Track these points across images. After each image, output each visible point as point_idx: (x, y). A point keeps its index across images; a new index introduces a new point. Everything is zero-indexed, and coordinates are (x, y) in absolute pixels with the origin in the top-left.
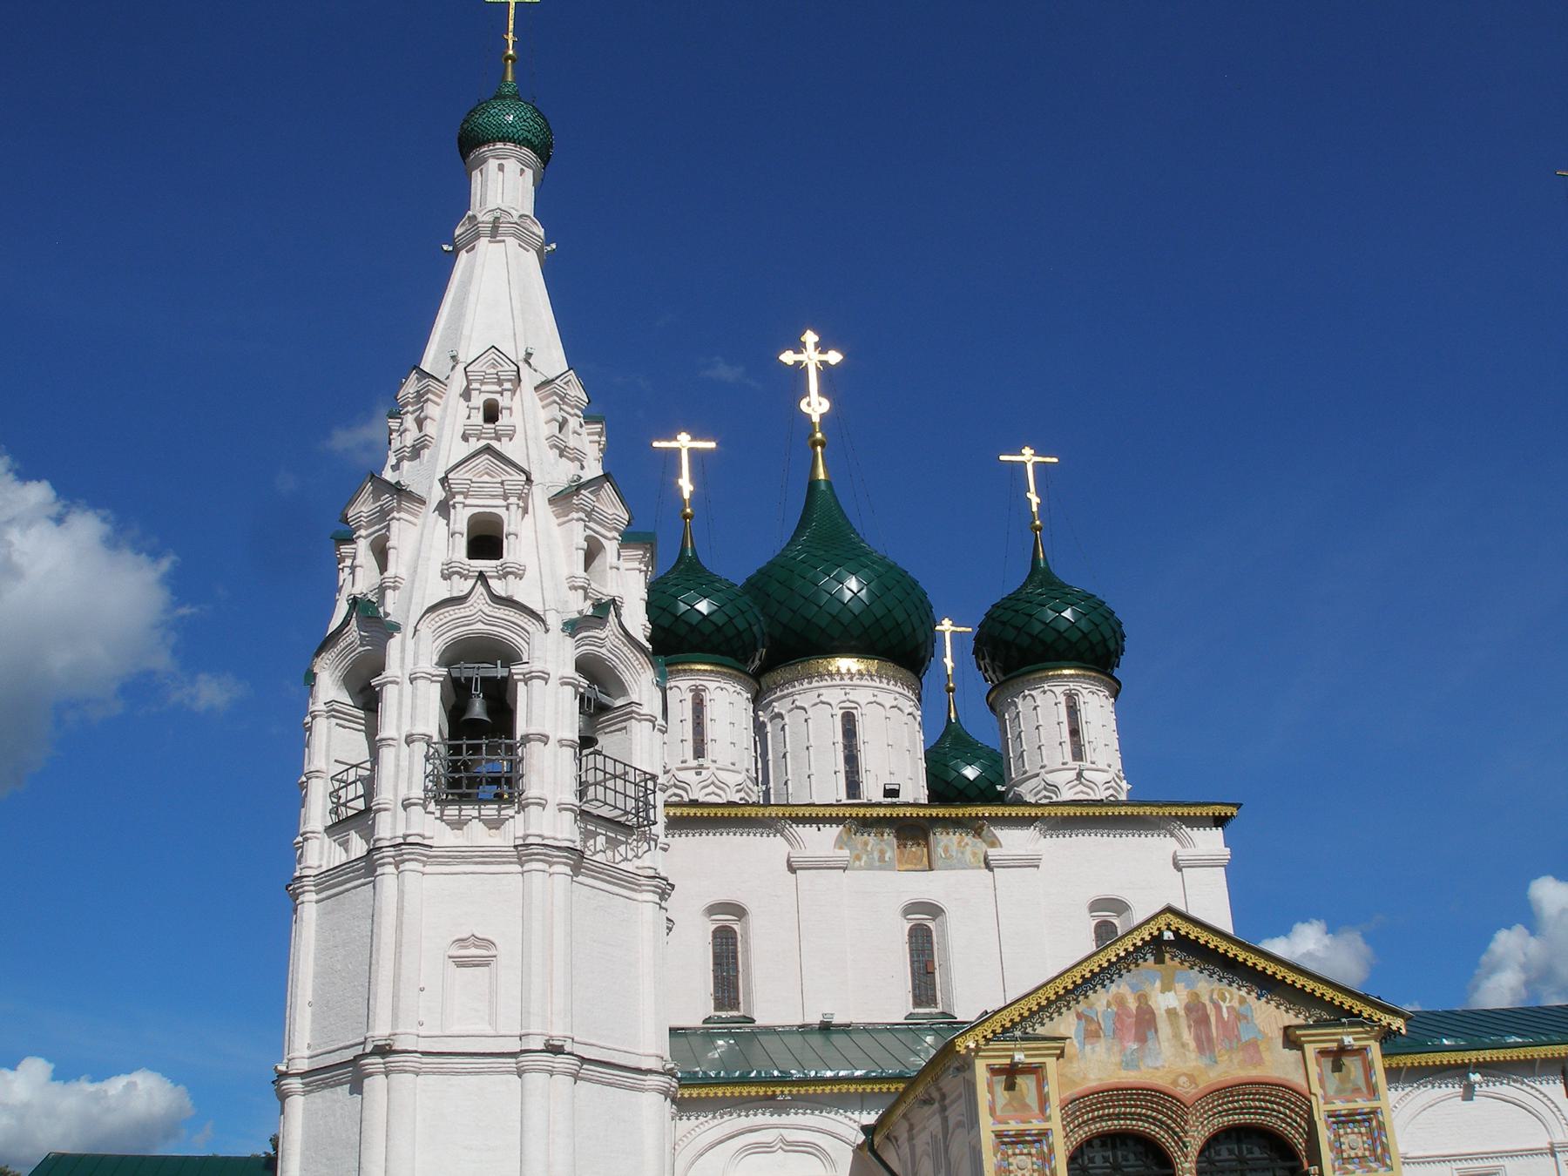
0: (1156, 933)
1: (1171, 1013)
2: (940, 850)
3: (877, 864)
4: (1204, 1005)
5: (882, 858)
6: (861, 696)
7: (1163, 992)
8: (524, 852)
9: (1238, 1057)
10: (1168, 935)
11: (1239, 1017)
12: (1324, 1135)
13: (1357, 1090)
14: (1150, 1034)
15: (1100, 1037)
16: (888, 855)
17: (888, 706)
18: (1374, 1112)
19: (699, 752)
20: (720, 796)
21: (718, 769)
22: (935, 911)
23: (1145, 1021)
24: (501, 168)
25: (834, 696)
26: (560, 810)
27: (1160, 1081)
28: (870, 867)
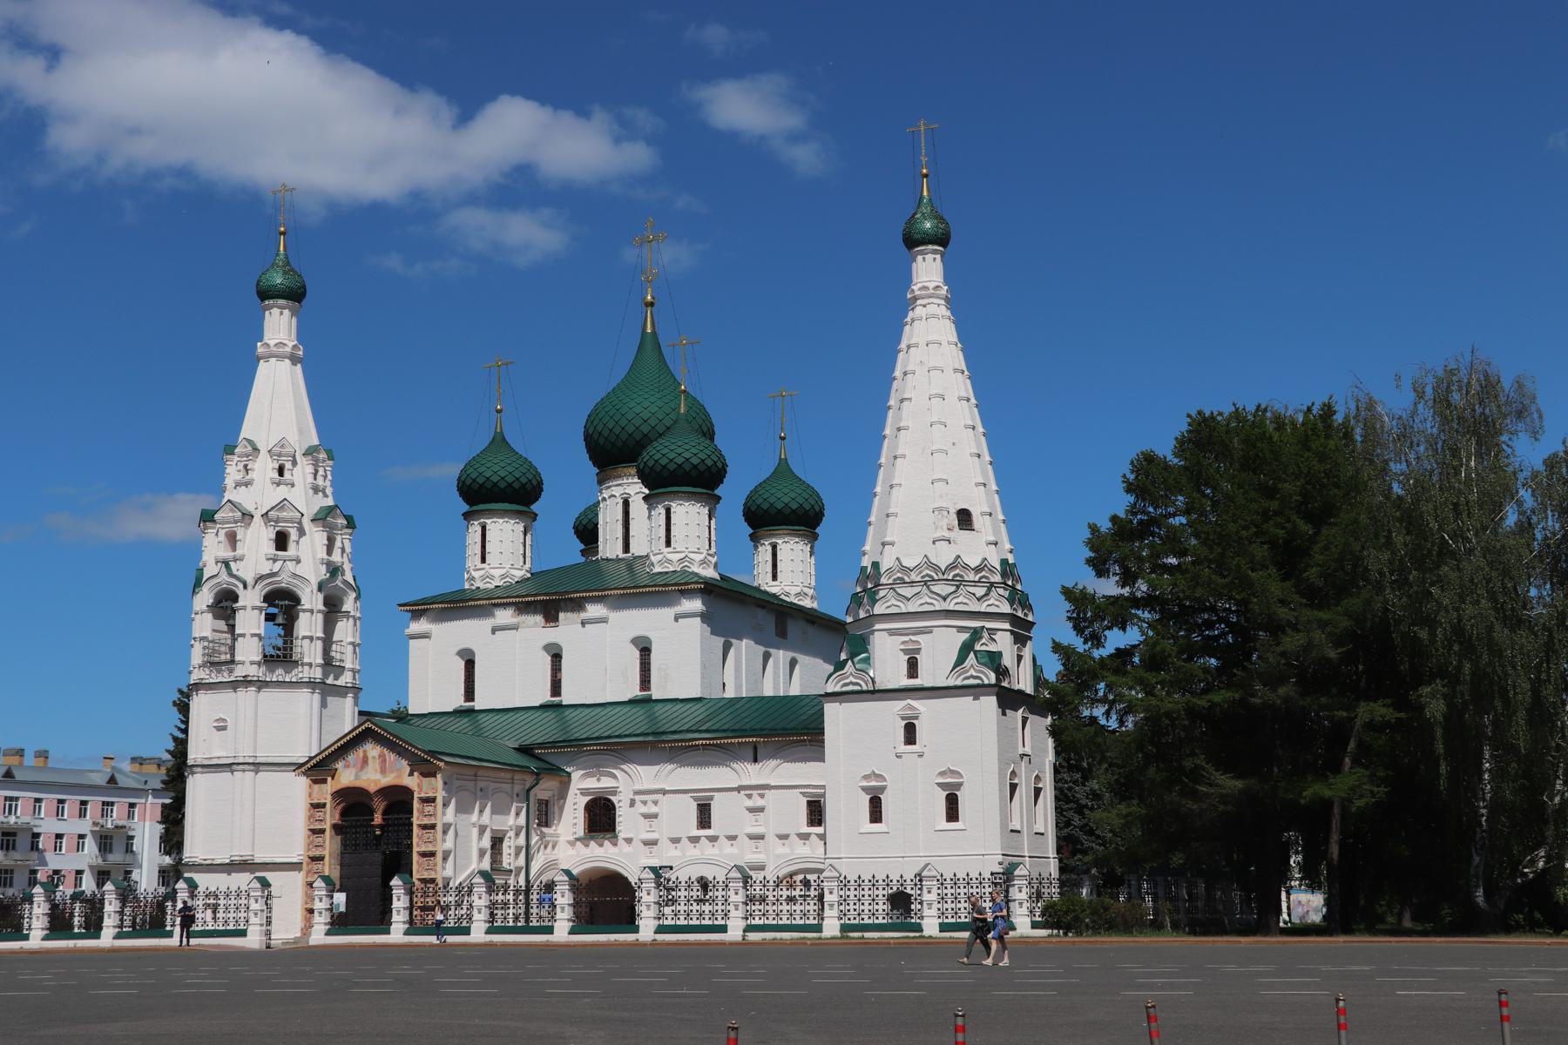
1: (374, 757)
2: (562, 615)
5: (536, 623)
7: (373, 749)
8: (234, 685)
9: (393, 776)
12: (416, 805)
20: (490, 583)
21: (490, 568)
23: (365, 761)
24: (270, 313)
25: (617, 491)
26: (251, 664)
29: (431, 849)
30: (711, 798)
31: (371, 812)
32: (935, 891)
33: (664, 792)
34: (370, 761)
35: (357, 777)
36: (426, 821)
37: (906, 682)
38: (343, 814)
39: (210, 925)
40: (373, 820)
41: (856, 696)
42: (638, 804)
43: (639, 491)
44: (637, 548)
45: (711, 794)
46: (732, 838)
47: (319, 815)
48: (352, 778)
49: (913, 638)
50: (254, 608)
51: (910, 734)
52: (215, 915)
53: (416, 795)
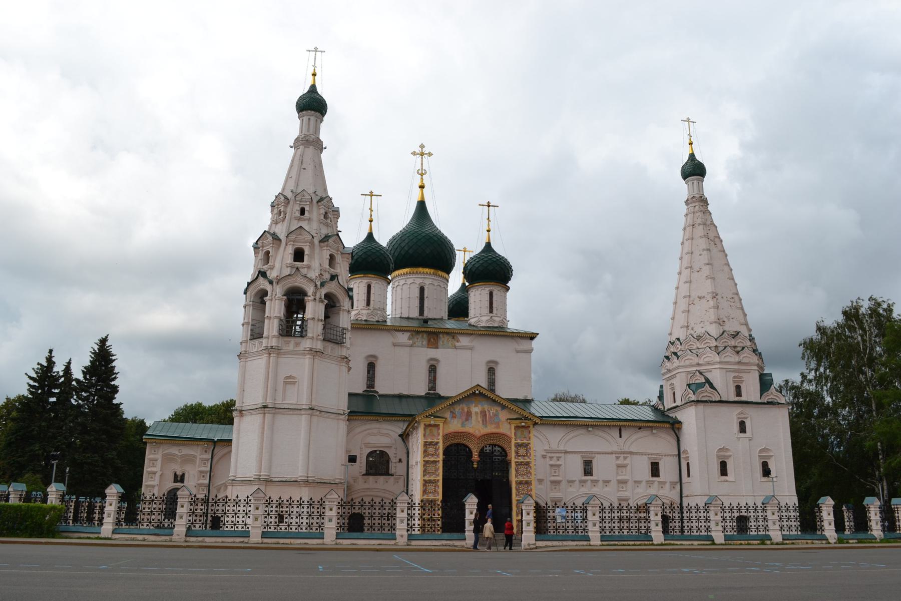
0: (474, 391)
1: (476, 413)
2: (441, 342)
3: (420, 344)
4: (486, 412)
5: (422, 345)
6: (427, 282)
7: (475, 407)
9: (493, 426)
10: (477, 392)
11: (496, 415)
13: (525, 437)
14: (470, 418)
15: (455, 418)
16: (424, 343)
17: (436, 284)
18: (529, 443)
19: (368, 304)
22: (437, 360)
23: (469, 415)
27: (471, 431)
28: (419, 347)
29: (526, 479)
30: (593, 458)
31: (470, 452)
32: (598, 515)
33: (566, 452)
34: (474, 417)
35: (463, 425)
36: (521, 460)
37: (737, 399)
38: (446, 452)
39: (580, 532)
40: (472, 458)
41: (735, 405)
42: (548, 458)
43: (431, 282)
44: (427, 314)
45: (593, 455)
46: (606, 482)
47: (431, 450)
48: (459, 425)
49: (741, 375)
50: (322, 301)
51: (742, 428)
52: (682, 524)
53: (513, 442)
